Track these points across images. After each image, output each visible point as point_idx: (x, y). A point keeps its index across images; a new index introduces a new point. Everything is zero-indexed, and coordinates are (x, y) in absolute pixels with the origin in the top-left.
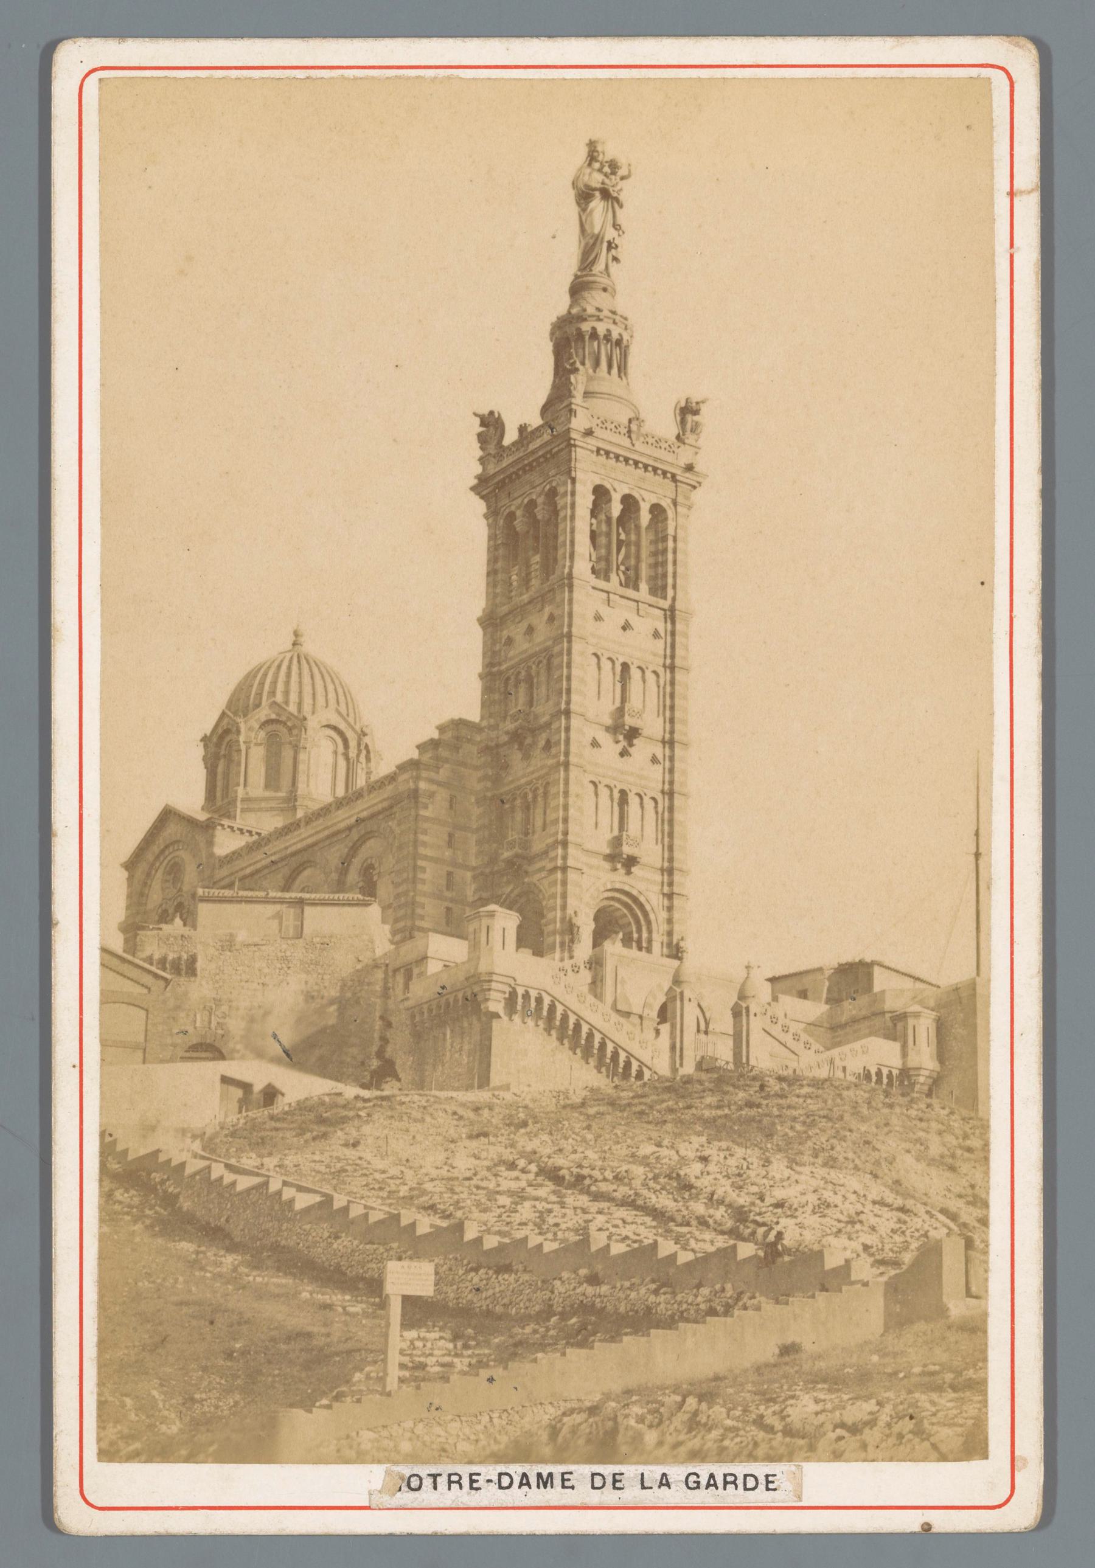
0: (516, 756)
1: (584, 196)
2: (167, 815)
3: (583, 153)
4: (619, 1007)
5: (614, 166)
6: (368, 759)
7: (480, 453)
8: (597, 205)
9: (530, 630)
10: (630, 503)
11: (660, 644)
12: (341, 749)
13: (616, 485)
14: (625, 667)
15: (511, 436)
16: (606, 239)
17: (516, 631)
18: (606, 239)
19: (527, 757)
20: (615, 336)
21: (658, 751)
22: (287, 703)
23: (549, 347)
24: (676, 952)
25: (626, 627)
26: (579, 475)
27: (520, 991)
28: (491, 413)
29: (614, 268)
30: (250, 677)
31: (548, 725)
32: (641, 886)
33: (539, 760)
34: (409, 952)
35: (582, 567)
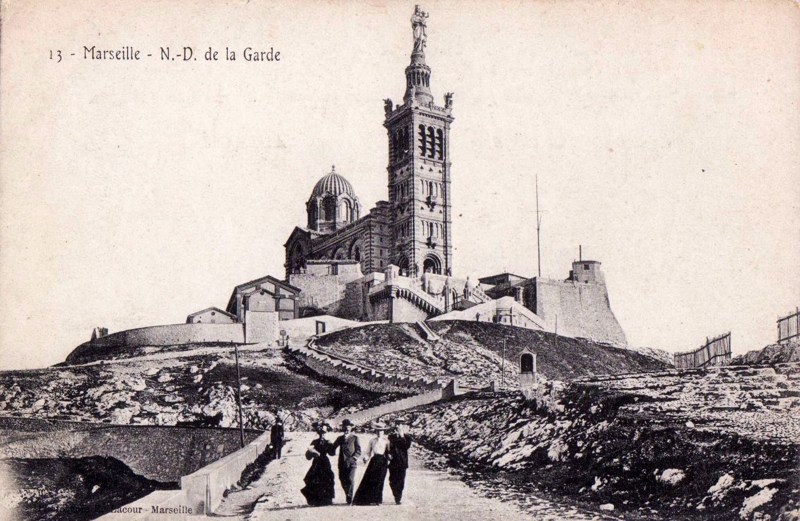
0: (399, 213)
1: (414, 25)
2: (297, 229)
3: (413, 11)
4: (431, 292)
5: (423, 14)
6: (358, 207)
7: (385, 113)
8: (418, 28)
9: (402, 172)
10: (431, 129)
11: (441, 175)
12: (348, 205)
13: (427, 124)
14: (431, 184)
15: (394, 108)
16: (422, 39)
17: (398, 172)
18: (422, 39)
19: (402, 212)
20: (425, 73)
21: (442, 209)
22: (331, 191)
23: (405, 76)
24: (448, 272)
25: (431, 170)
26: (415, 122)
27: (400, 290)
28: (388, 99)
29: (424, 49)
30: (320, 182)
31: (408, 203)
32: (437, 252)
33: (406, 214)
34: (368, 278)
35: (417, 152)
